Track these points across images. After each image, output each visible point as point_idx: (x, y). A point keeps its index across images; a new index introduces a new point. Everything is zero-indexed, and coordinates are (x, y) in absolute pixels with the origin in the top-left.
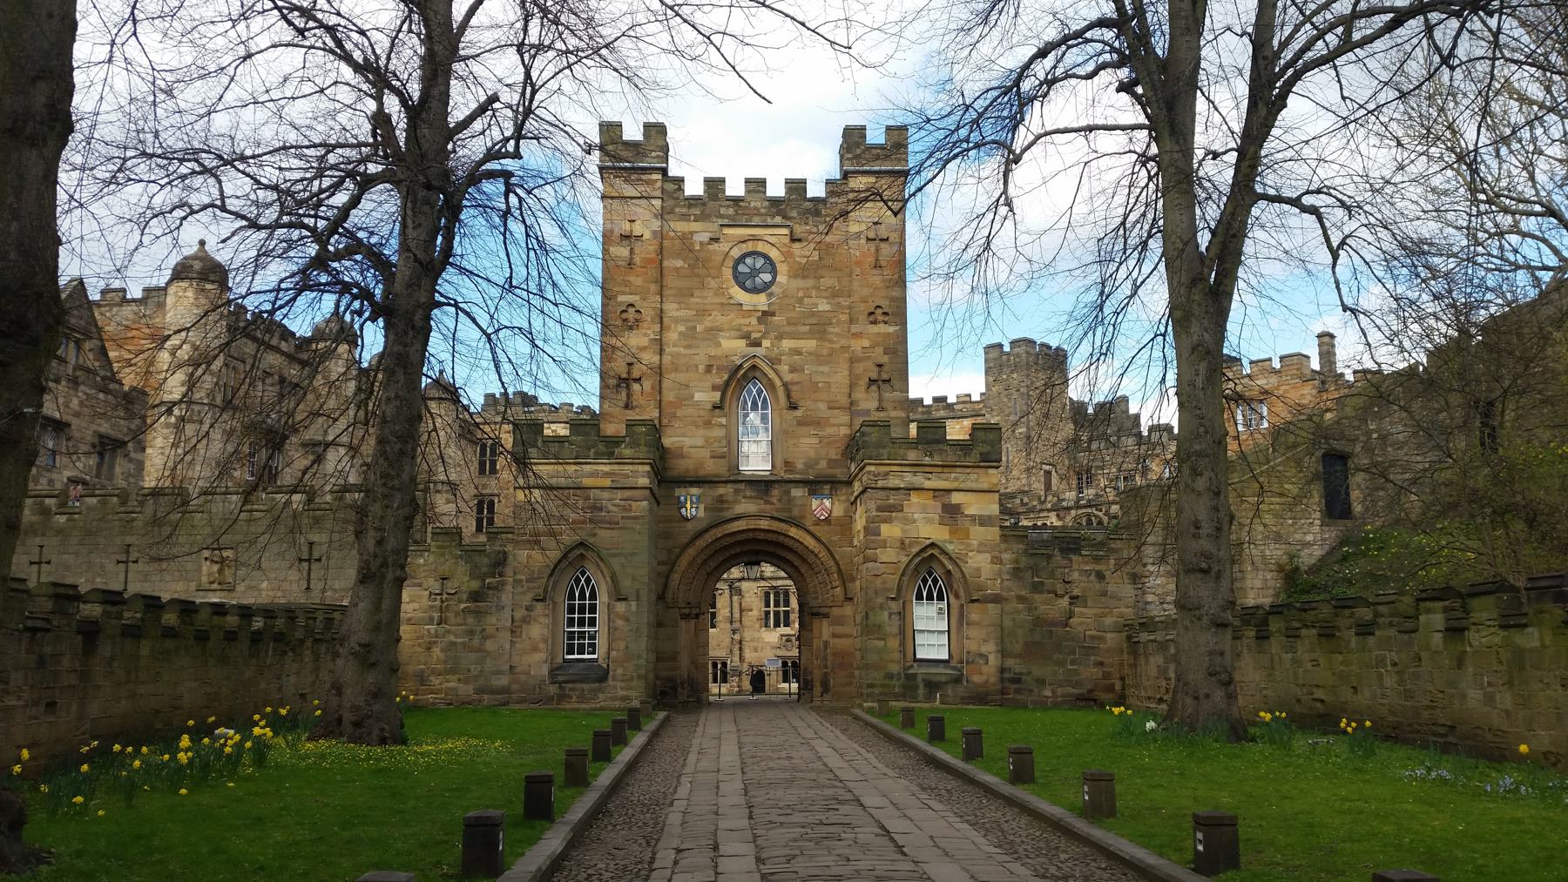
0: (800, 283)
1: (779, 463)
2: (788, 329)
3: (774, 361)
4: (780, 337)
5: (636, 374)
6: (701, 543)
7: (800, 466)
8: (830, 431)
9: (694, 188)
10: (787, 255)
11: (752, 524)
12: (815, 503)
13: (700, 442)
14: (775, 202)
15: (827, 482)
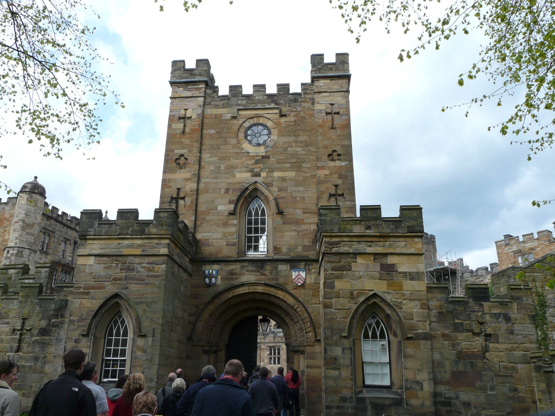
0: (286, 139)
1: (271, 249)
2: (278, 166)
3: (268, 185)
4: (271, 171)
5: (182, 195)
6: (218, 302)
7: (284, 250)
8: (304, 227)
9: (224, 91)
10: (278, 124)
11: (252, 289)
12: (294, 274)
13: (219, 235)
14: (271, 96)
15: (301, 261)
